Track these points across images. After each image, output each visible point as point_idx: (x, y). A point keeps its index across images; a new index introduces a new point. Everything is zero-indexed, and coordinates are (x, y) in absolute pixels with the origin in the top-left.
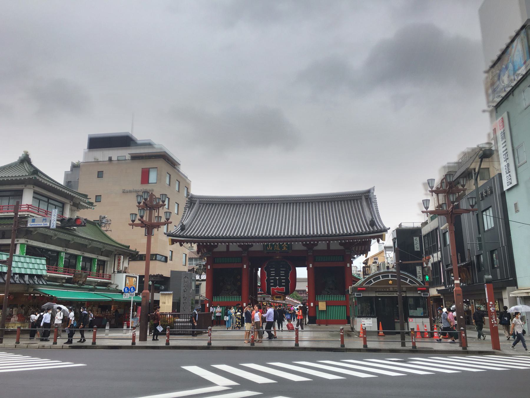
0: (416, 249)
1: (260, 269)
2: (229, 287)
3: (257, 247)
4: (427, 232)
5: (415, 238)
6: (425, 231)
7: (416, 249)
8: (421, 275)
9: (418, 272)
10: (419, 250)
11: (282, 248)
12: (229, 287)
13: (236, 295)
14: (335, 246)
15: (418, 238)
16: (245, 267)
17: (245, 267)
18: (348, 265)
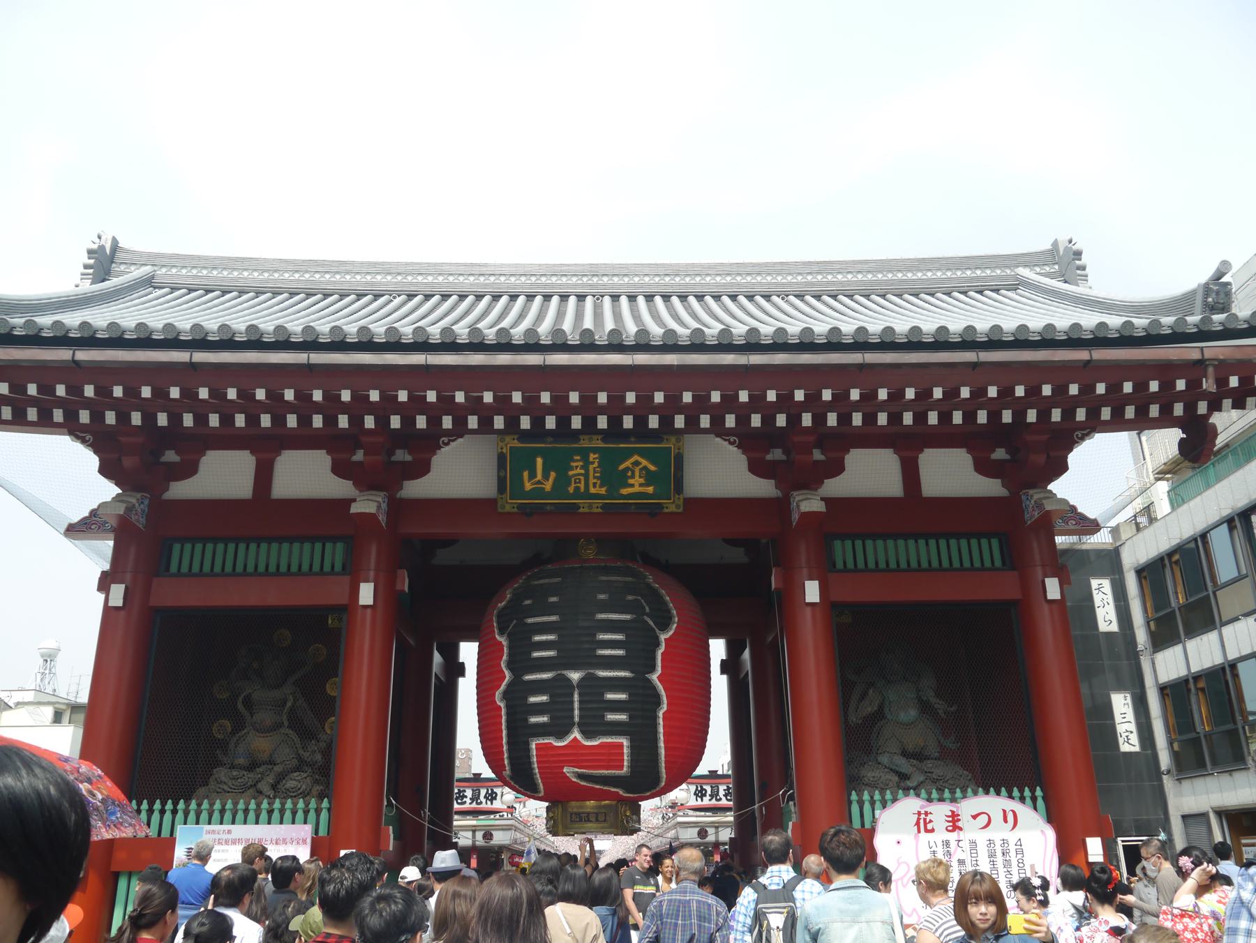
0: (1103, 627)
1: (469, 652)
2: (262, 744)
3: (460, 472)
4: (1175, 542)
5: (1095, 583)
6: (1138, 552)
7: (1103, 627)
8: (1133, 727)
9: (1118, 718)
10: (1114, 628)
11: (623, 479)
12: (262, 744)
13: (305, 795)
14: (950, 474)
15: (1106, 584)
16: (366, 594)
17: (366, 594)
18: (1053, 589)
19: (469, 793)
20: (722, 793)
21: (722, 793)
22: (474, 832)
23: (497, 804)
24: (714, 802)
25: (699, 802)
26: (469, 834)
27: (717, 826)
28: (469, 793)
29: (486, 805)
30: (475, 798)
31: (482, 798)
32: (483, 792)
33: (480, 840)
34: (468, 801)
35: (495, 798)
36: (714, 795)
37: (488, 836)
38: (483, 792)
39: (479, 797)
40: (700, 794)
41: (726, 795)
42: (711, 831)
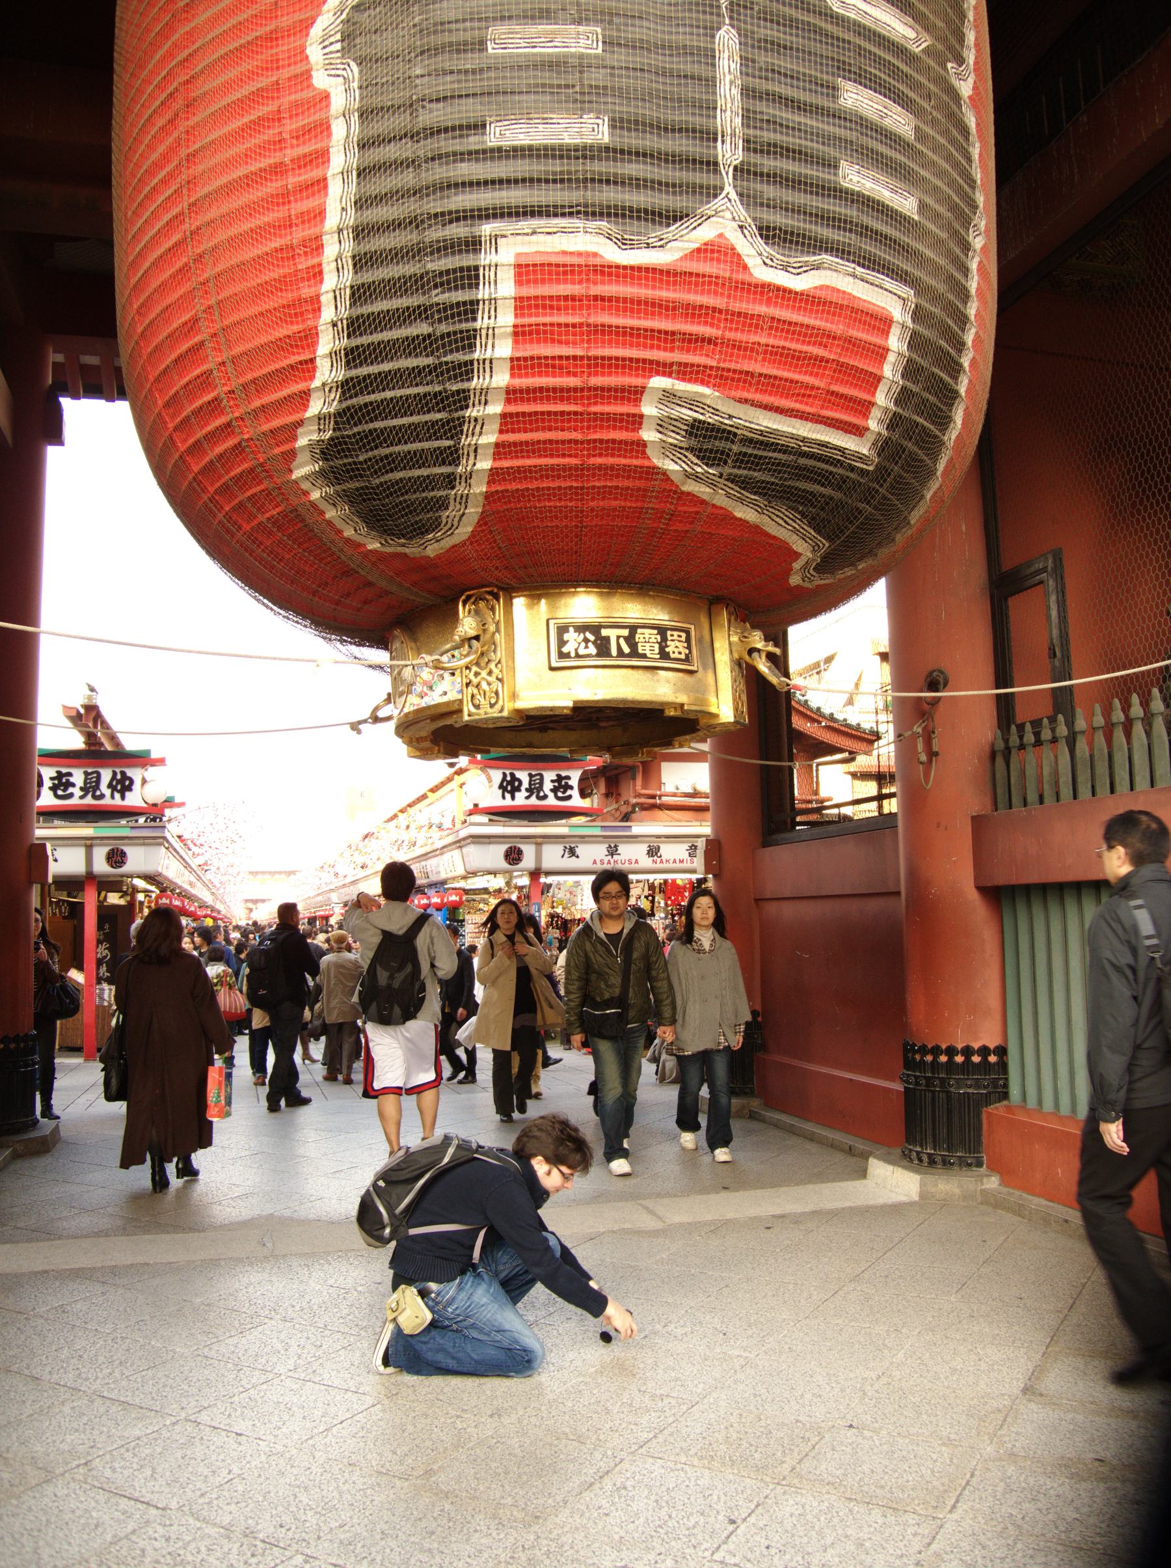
19: (78, 777)
20: (548, 786)
21: (548, 786)
22: (89, 849)
23: (133, 799)
24: (533, 801)
25: (508, 802)
26: (81, 852)
27: (539, 841)
28: (78, 777)
29: (111, 800)
30: (91, 787)
31: (104, 788)
32: (106, 775)
33: (101, 866)
34: (77, 792)
35: (129, 788)
36: (535, 789)
37: (116, 857)
38: (106, 775)
39: (97, 786)
40: (510, 786)
41: (554, 790)
42: (528, 851)
